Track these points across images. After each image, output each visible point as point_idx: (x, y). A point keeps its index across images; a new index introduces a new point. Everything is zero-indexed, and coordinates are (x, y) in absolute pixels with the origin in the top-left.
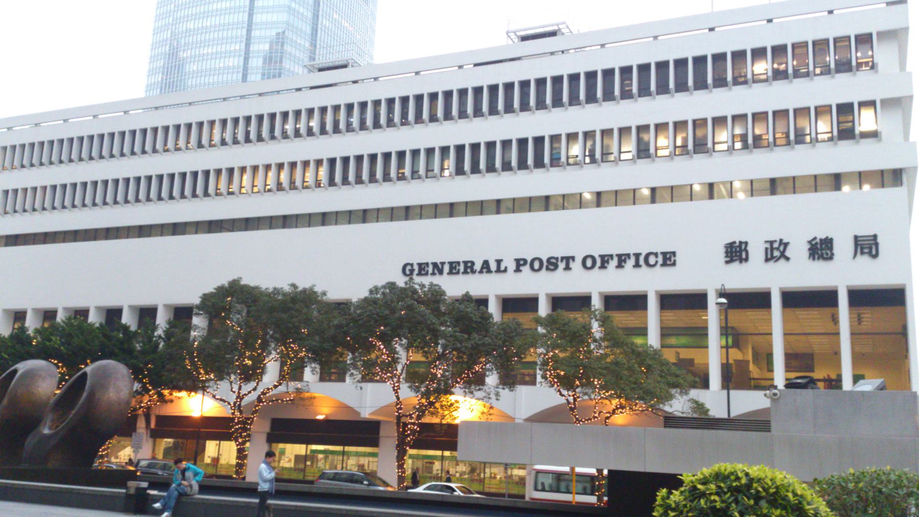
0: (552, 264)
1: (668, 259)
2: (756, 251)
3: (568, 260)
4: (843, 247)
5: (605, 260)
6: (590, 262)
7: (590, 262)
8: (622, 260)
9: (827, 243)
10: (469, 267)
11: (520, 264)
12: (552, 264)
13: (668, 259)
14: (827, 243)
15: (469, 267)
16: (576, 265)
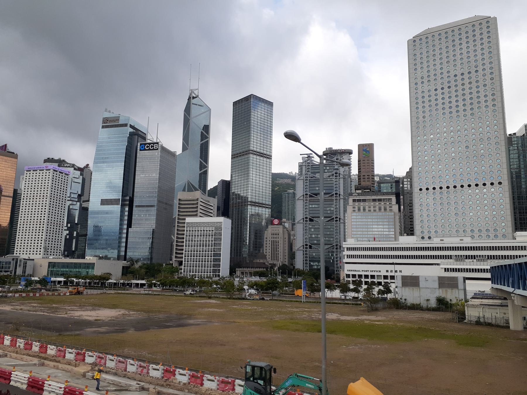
0: (366, 271)
1: (380, 271)
2: (389, 271)
3: (368, 271)
4: (398, 271)
5: (373, 271)
6: (371, 271)
7: (371, 271)
8: (375, 271)
9: (397, 271)
10: (356, 271)
11: (362, 271)
12: (366, 271)
13: (380, 271)
14: (397, 271)
15: (356, 271)
16: (369, 271)
